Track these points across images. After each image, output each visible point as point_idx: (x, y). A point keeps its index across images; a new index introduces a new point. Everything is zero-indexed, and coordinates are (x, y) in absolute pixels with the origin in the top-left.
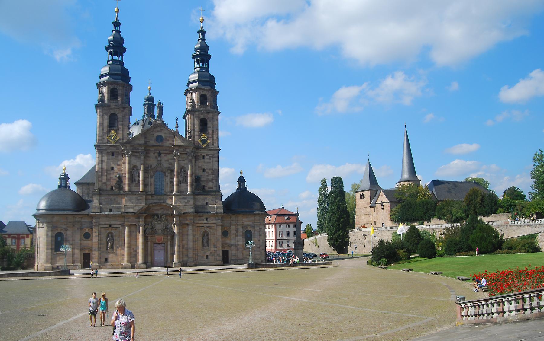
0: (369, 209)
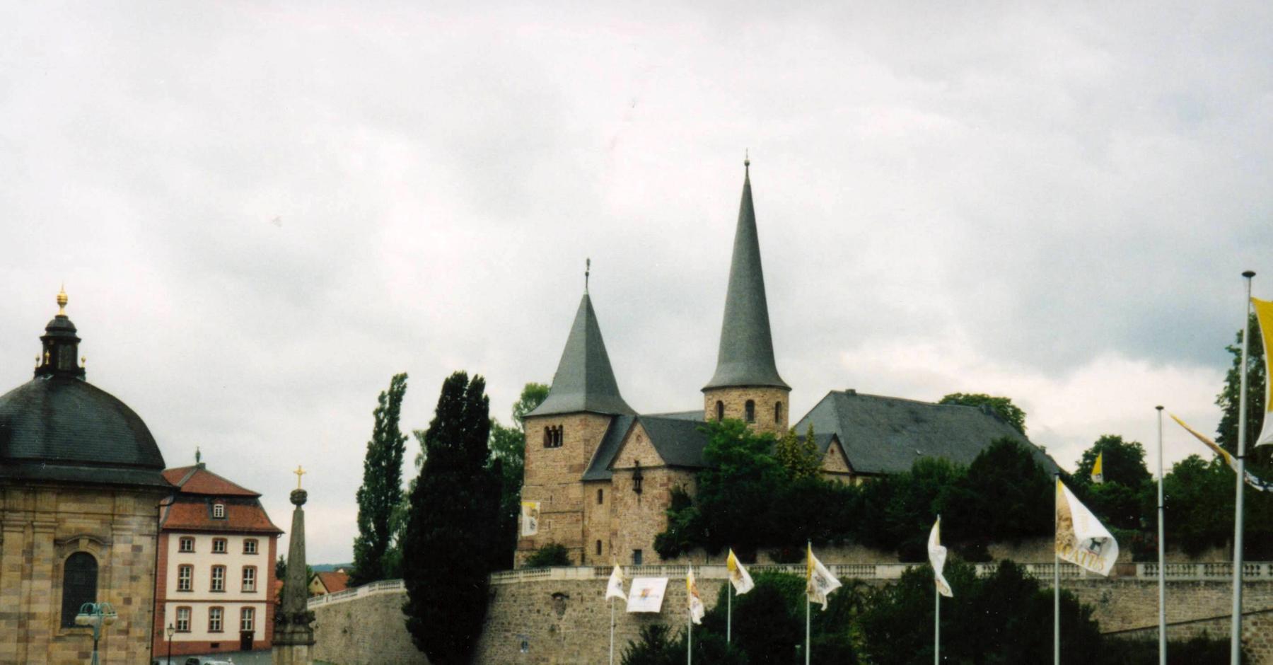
0: (576, 492)
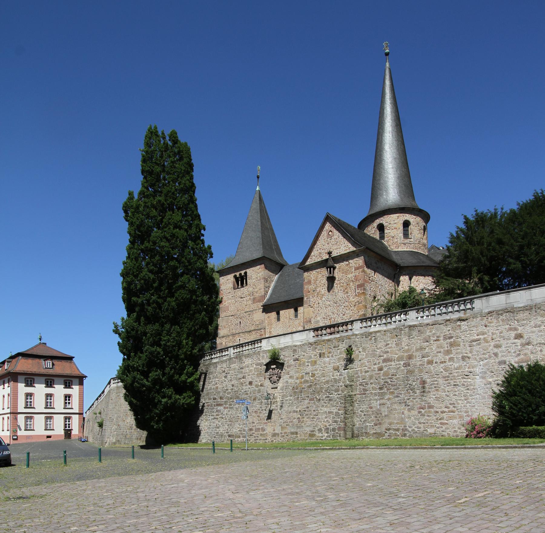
0: (259, 315)
